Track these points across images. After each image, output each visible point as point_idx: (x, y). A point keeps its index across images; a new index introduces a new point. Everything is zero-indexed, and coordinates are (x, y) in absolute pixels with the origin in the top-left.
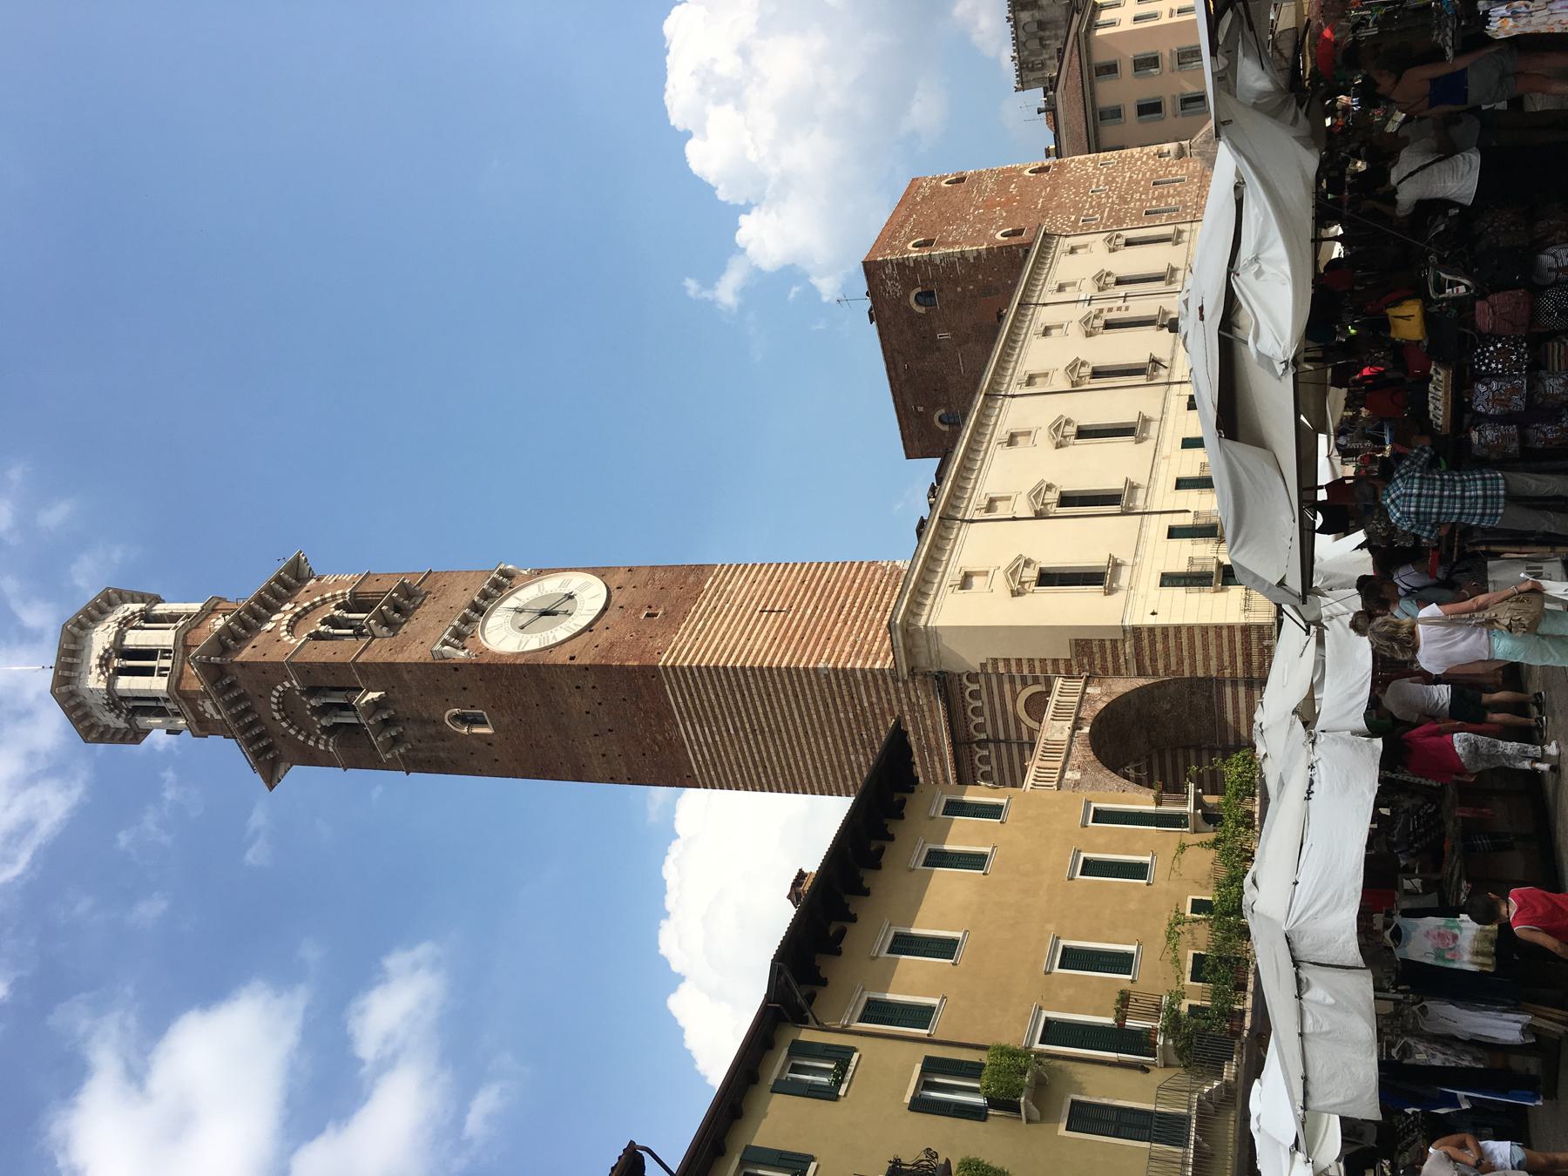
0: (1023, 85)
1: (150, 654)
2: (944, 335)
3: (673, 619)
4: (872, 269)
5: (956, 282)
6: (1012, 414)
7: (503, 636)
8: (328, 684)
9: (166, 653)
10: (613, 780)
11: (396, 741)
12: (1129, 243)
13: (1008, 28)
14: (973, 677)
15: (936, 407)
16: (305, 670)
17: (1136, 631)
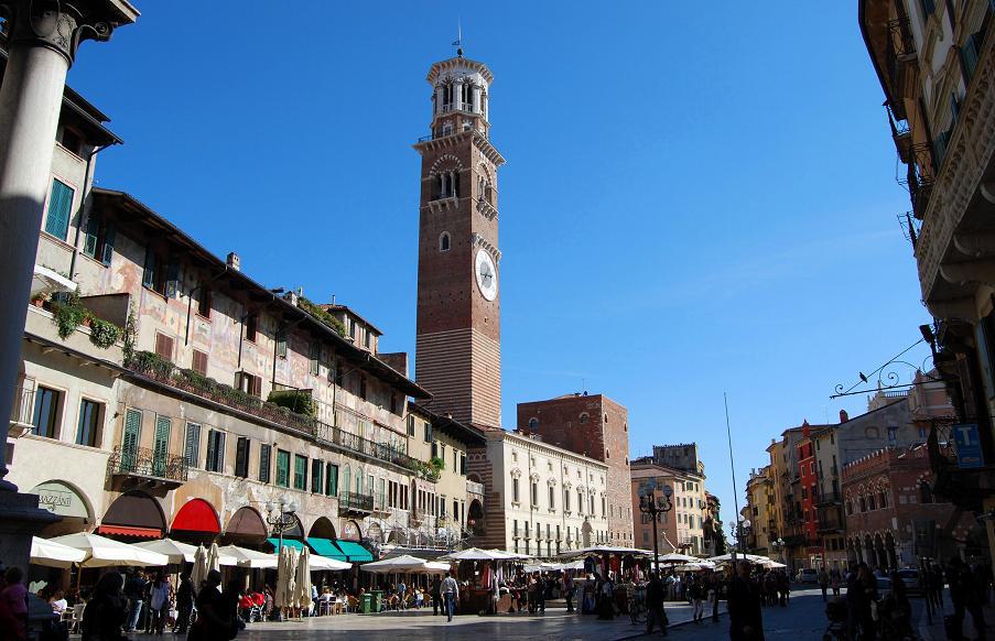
0: (655, 449)
1: (470, 101)
2: (570, 424)
3: (484, 330)
4: (598, 398)
5: (591, 431)
6: (556, 461)
7: (481, 258)
8: (461, 183)
9: (471, 109)
10: (419, 299)
11: (435, 207)
12: (603, 500)
13: (678, 444)
14: (484, 457)
15: (540, 419)
16: (468, 175)
17: (503, 513)
